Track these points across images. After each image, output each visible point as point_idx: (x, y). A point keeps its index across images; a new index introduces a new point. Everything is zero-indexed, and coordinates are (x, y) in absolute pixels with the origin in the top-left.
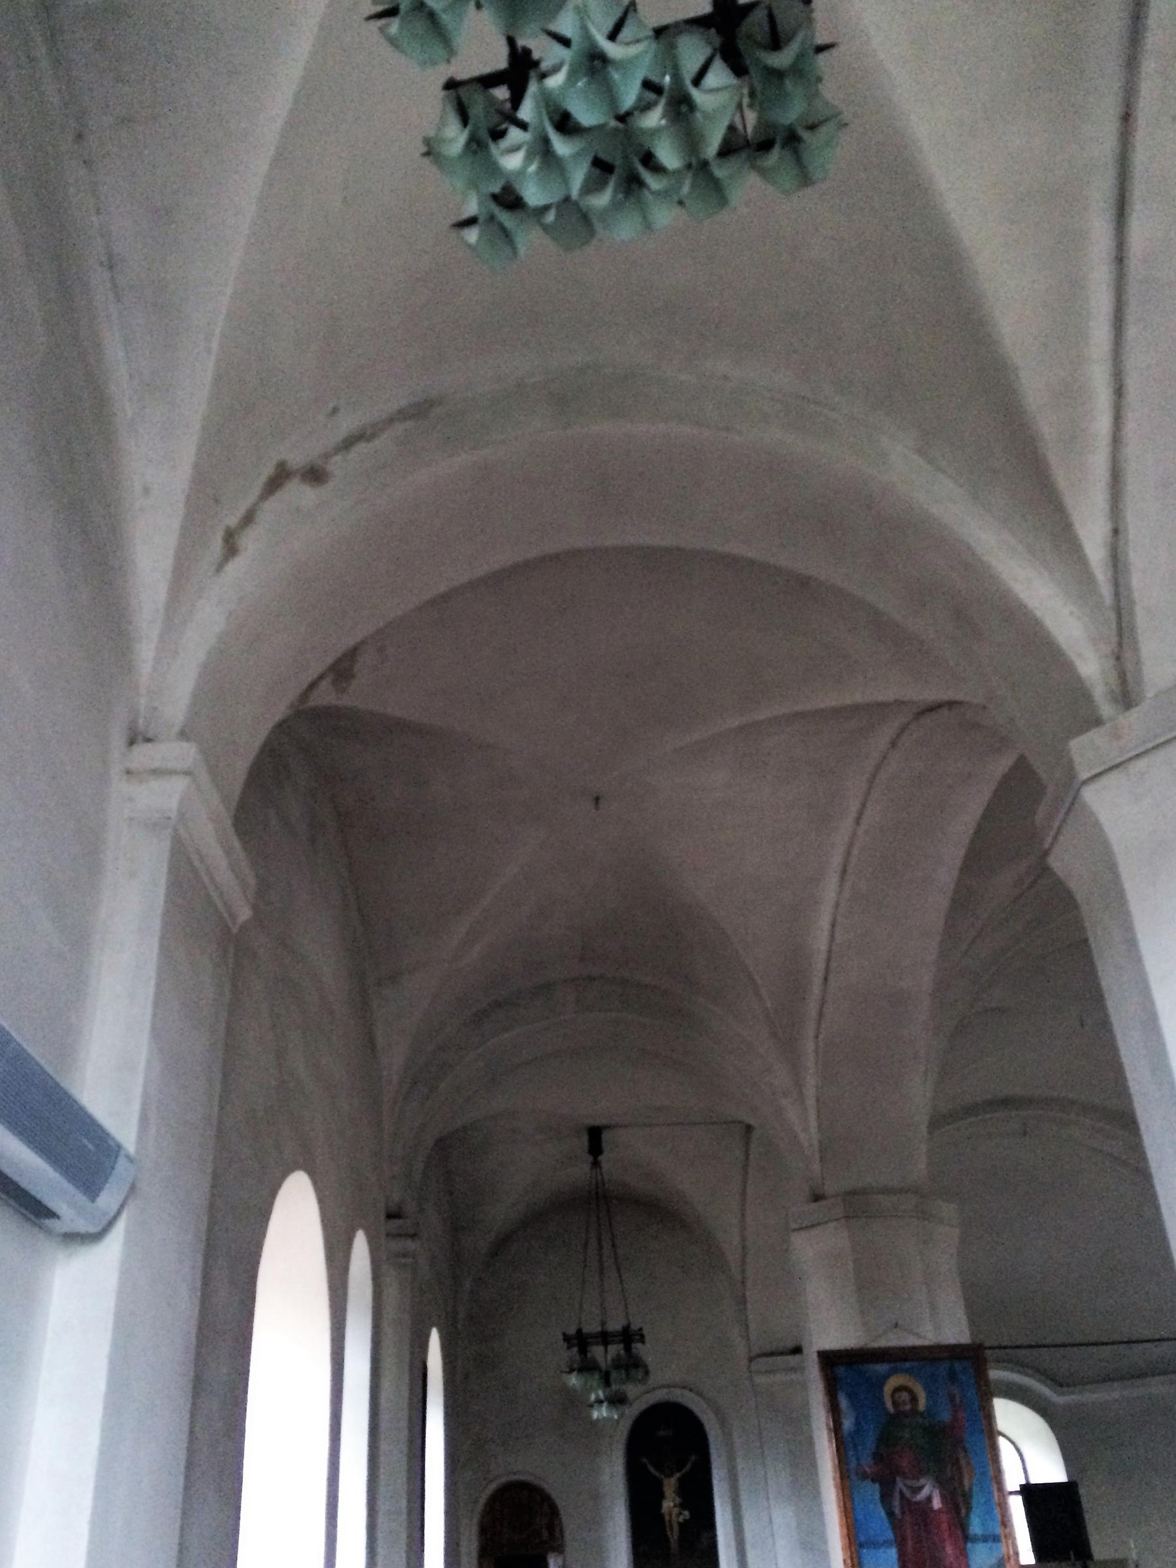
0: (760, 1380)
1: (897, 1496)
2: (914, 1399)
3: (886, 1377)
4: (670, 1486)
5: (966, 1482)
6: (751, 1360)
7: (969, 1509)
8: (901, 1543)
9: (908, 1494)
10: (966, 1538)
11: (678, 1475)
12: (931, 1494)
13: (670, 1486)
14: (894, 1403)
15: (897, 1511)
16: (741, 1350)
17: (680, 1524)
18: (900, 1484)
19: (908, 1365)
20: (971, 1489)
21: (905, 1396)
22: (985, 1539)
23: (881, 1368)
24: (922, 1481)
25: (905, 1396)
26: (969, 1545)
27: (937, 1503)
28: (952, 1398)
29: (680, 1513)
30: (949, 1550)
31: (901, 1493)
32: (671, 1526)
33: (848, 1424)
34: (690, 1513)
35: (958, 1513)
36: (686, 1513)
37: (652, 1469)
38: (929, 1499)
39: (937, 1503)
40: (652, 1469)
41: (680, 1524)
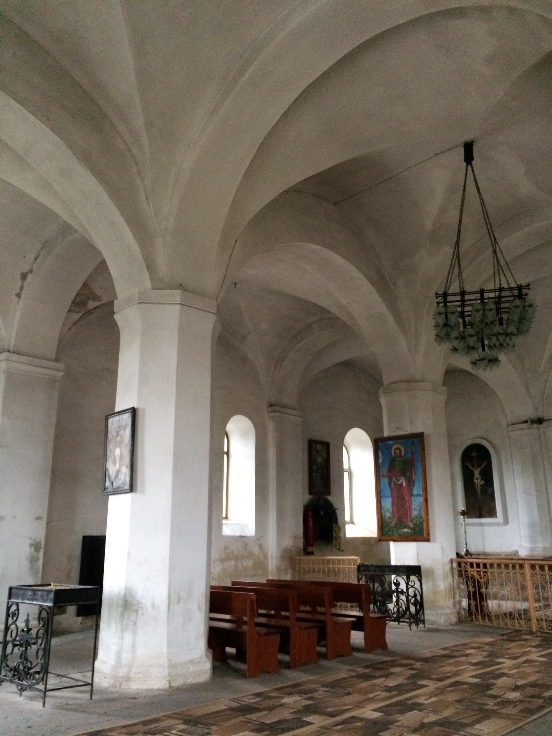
0: (511, 434)
1: (393, 483)
2: (401, 452)
3: (392, 446)
4: (477, 473)
5: (414, 478)
6: (508, 426)
7: (413, 487)
8: (393, 498)
9: (396, 481)
10: (411, 495)
11: (479, 469)
12: (403, 481)
13: (477, 473)
14: (395, 453)
15: (392, 487)
16: (504, 422)
18: (394, 479)
19: (400, 441)
20: (415, 480)
21: (398, 451)
22: (418, 495)
23: (391, 442)
24: (401, 478)
25: (398, 451)
26: (413, 497)
27: (404, 485)
28: (412, 451)
29: (481, 482)
30: (407, 499)
31: (394, 482)
32: (478, 486)
33: (381, 461)
35: (410, 487)
37: (470, 467)
38: (402, 484)
39: (404, 485)
40: (470, 467)
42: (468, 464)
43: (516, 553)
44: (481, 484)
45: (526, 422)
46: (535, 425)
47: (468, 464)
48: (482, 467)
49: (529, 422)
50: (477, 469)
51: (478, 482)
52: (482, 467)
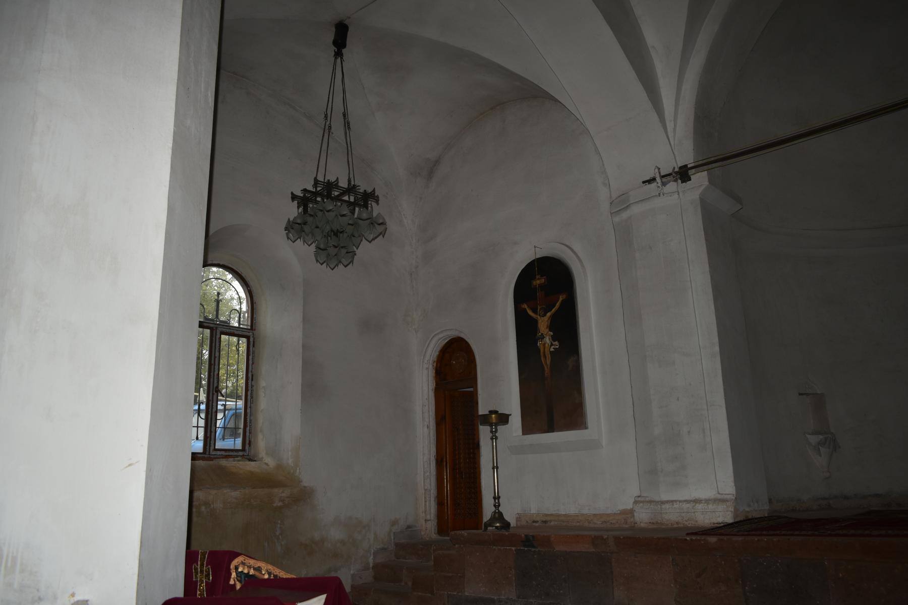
4: (543, 324)
11: (549, 314)
13: (543, 324)
17: (551, 353)
29: (552, 345)
34: (559, 342)
36: (557, 343)
37: (530, 313)
40: (530, 313)
41: (551, 353)
42: (525, 306)
43: (631, 512)
44: (552, 350)
45: (652, 180)
46: (672, 186)
47: (525, 306)
48: (554, 310)
49: (658, 179)
50: (545, 315)
51: (547, 342)
52: (554, 310)
